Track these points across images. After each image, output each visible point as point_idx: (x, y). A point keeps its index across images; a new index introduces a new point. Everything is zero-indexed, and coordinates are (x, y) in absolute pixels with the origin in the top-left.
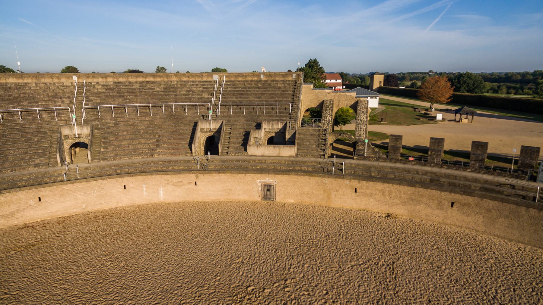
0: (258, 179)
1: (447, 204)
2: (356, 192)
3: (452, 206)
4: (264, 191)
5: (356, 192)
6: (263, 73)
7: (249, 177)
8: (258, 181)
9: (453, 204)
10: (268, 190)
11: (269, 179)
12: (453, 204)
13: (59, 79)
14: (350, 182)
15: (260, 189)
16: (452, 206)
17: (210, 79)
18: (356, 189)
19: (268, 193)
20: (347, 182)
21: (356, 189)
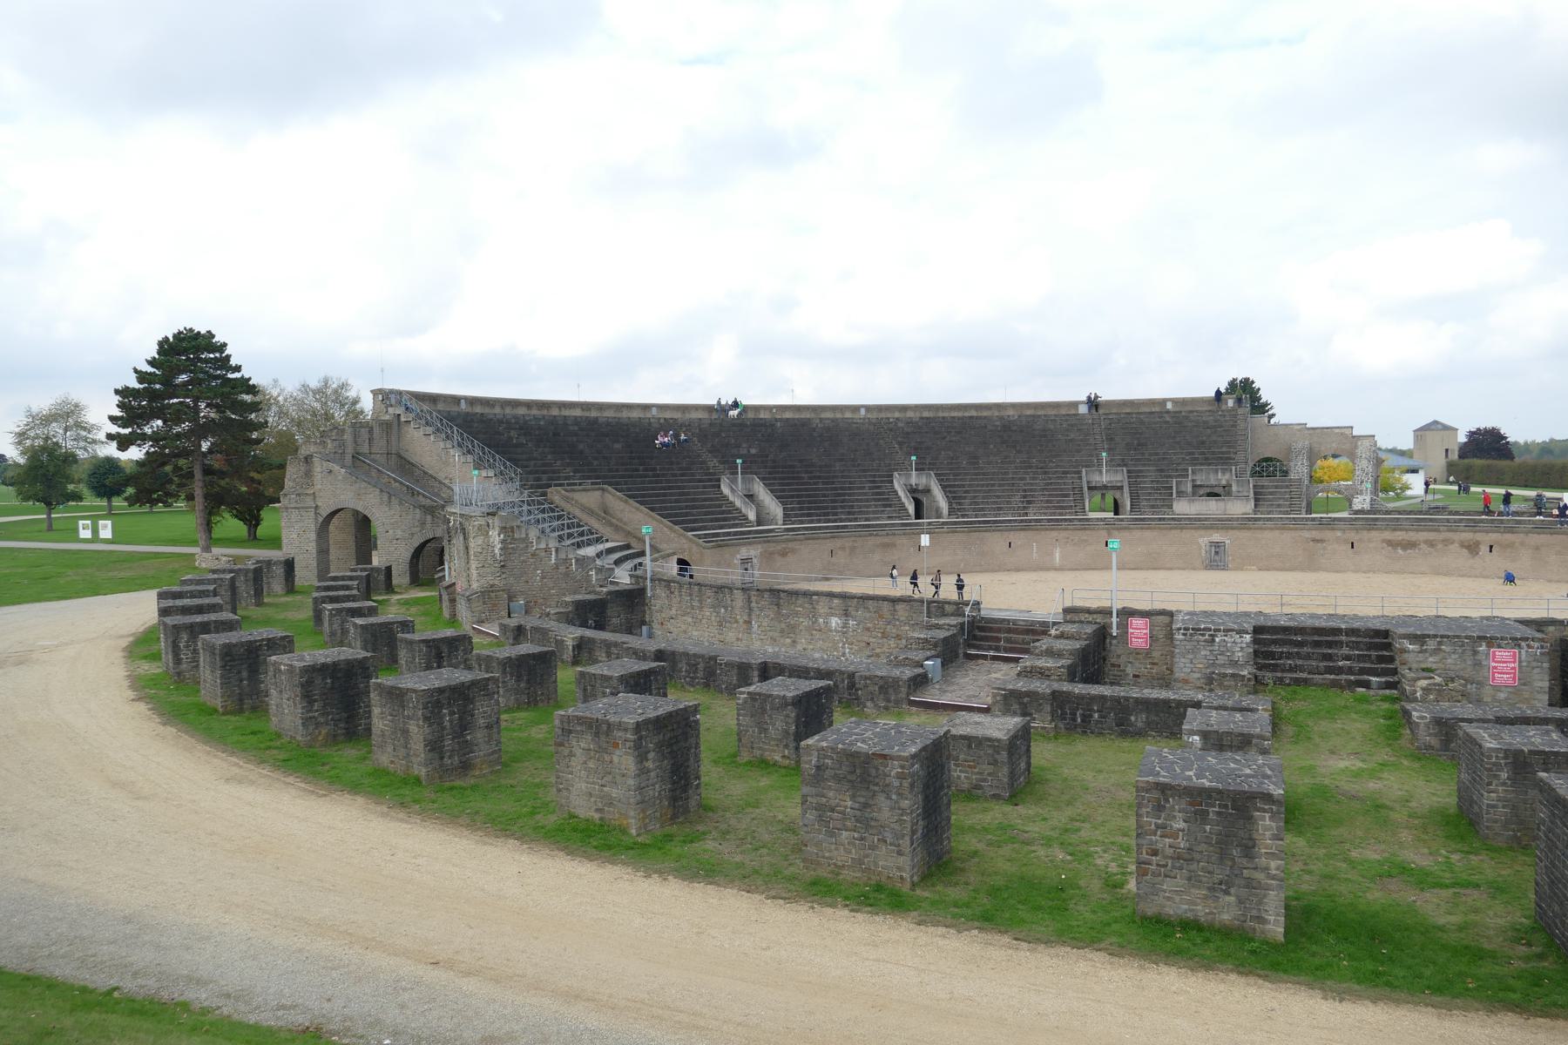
0: (1201, 536)
1: (1484, 549)
2: (1353, 547)
3: (1491, 551)
4: (1210, 554)
5: (1353, 547)
6: (1173, 400)
7: (1187, 535)
8: (1201, 540)
9: (1491, 547)
10: (1217, 553)
11: (1217, 537)
12: (1491, 547)
13: (843, 414)
14: (1344, 533)
15: (1204, 552)
16: (1491, 551)
17: (1073, 412)
18: (1352, 543)
19: (1217, 558)
20: (1339, 534)
21: (1352, 543)
